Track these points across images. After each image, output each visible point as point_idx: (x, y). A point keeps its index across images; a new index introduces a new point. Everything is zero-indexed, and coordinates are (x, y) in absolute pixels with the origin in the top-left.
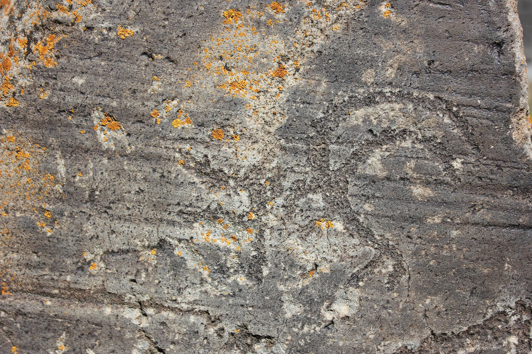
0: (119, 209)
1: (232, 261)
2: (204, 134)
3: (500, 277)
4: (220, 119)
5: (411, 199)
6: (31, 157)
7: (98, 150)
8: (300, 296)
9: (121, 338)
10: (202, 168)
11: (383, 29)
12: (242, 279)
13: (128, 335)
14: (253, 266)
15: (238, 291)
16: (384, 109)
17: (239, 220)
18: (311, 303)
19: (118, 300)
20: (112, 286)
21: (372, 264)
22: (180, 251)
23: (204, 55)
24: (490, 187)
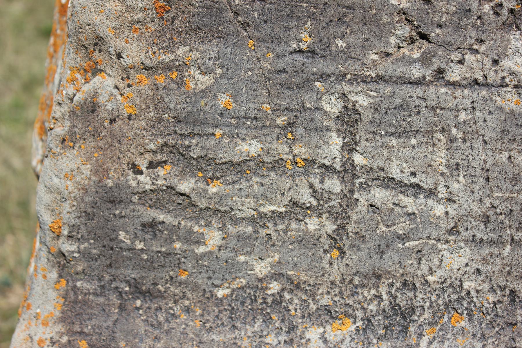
9: (376, 22)
13: (386, 19)
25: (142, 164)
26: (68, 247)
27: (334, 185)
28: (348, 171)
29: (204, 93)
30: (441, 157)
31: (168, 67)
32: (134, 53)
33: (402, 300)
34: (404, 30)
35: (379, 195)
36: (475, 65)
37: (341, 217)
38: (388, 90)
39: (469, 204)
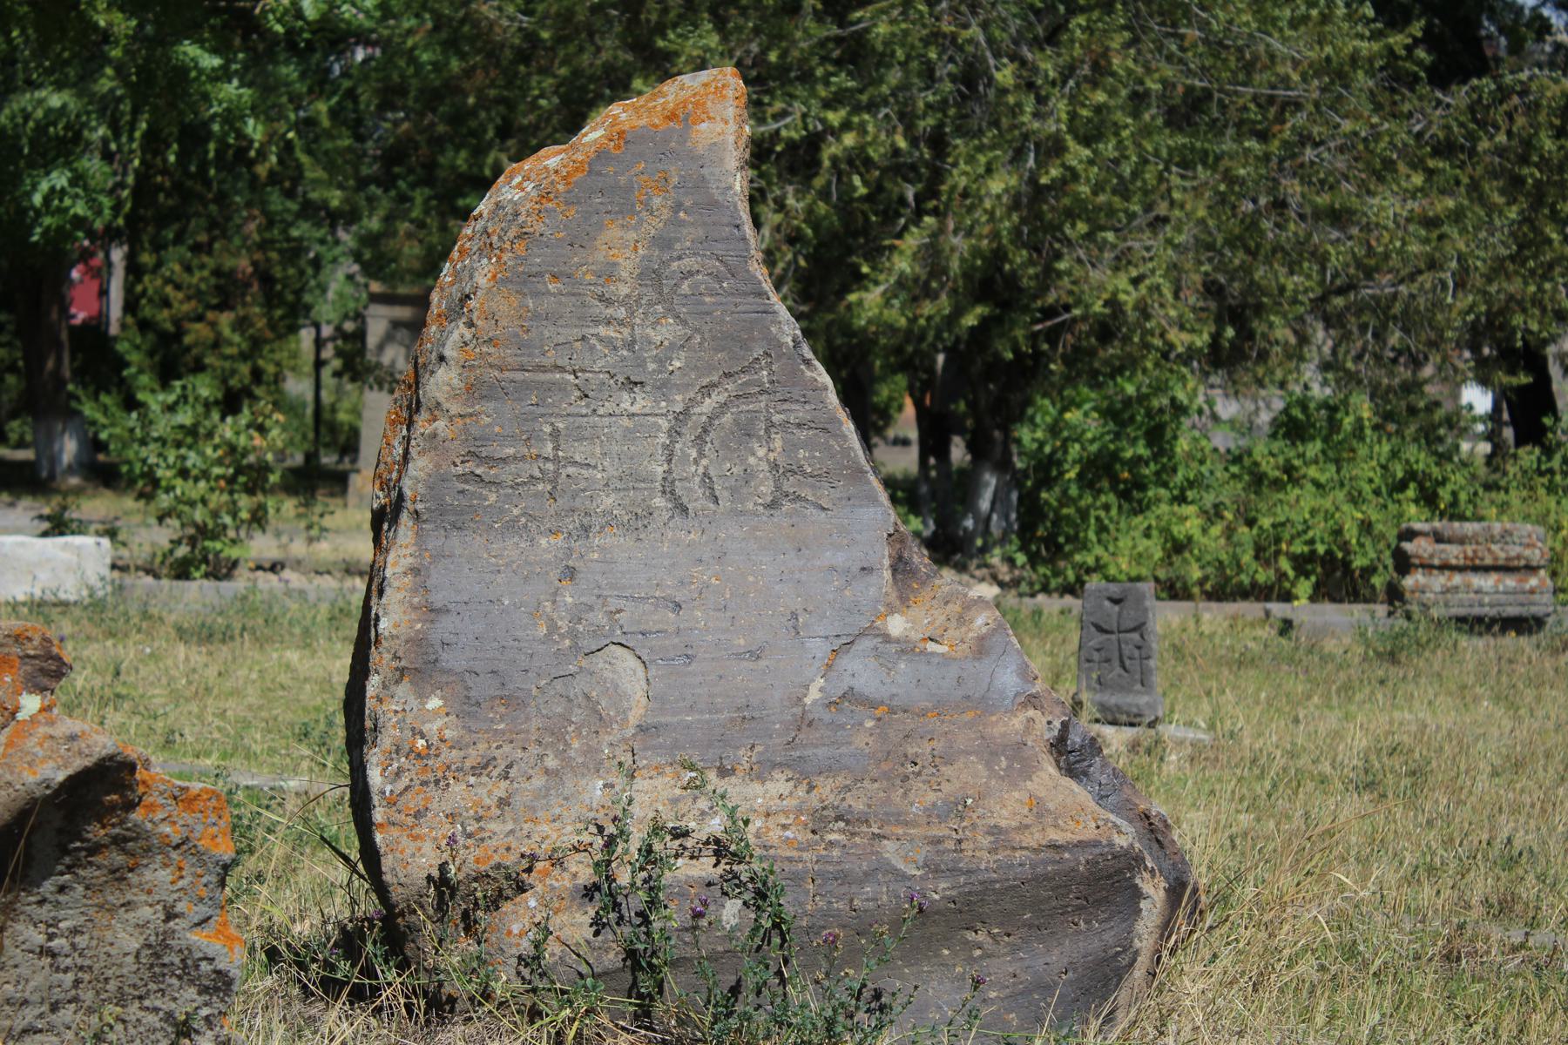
0: (561, 322)
1: (619, 344)
2: (601, 281)
3: (752, 339)
4: (609, 273)
5: (704, 303)
6: (515, 300)
7: (548, 292)
8: (656, 359)
10: (601, 298)
11: (682, 223)
12: (625, 353)
14: (630, 345)
15: (623, 359)
16: (686, 261)
17: (621, 323)
18: (661, 361)
19: (562, 369)
20: (559, 363)
21: (689, 338)
22: (593, 341)
23: (598, 243)
24: (746, 294)
25: (458, 461)
26: (419, 506)
27: (550, 466)
28: (556, 460)
29: (489, 425)
30: (598, 450)
31: (471, 415)
32: (455, 409)
33: (586, 521)
34: (578, 393)
35: (571, 470)
36: (609, 407)
37: (554, 481)
38: (571, 419)
39: (612, 471)
